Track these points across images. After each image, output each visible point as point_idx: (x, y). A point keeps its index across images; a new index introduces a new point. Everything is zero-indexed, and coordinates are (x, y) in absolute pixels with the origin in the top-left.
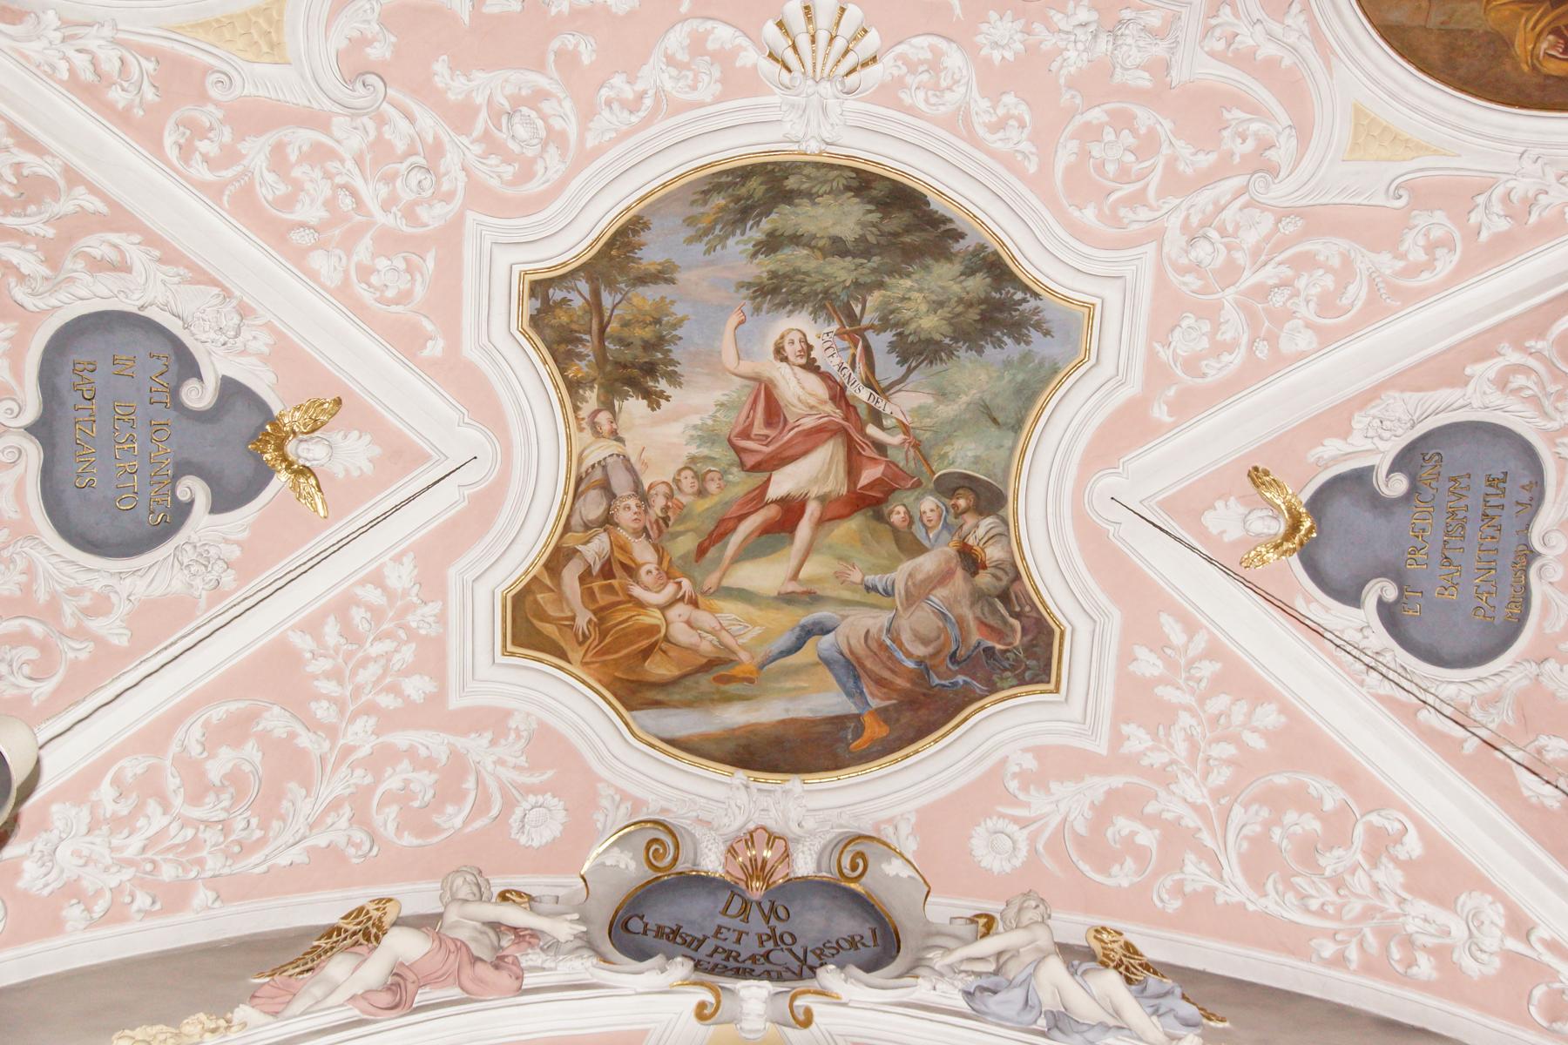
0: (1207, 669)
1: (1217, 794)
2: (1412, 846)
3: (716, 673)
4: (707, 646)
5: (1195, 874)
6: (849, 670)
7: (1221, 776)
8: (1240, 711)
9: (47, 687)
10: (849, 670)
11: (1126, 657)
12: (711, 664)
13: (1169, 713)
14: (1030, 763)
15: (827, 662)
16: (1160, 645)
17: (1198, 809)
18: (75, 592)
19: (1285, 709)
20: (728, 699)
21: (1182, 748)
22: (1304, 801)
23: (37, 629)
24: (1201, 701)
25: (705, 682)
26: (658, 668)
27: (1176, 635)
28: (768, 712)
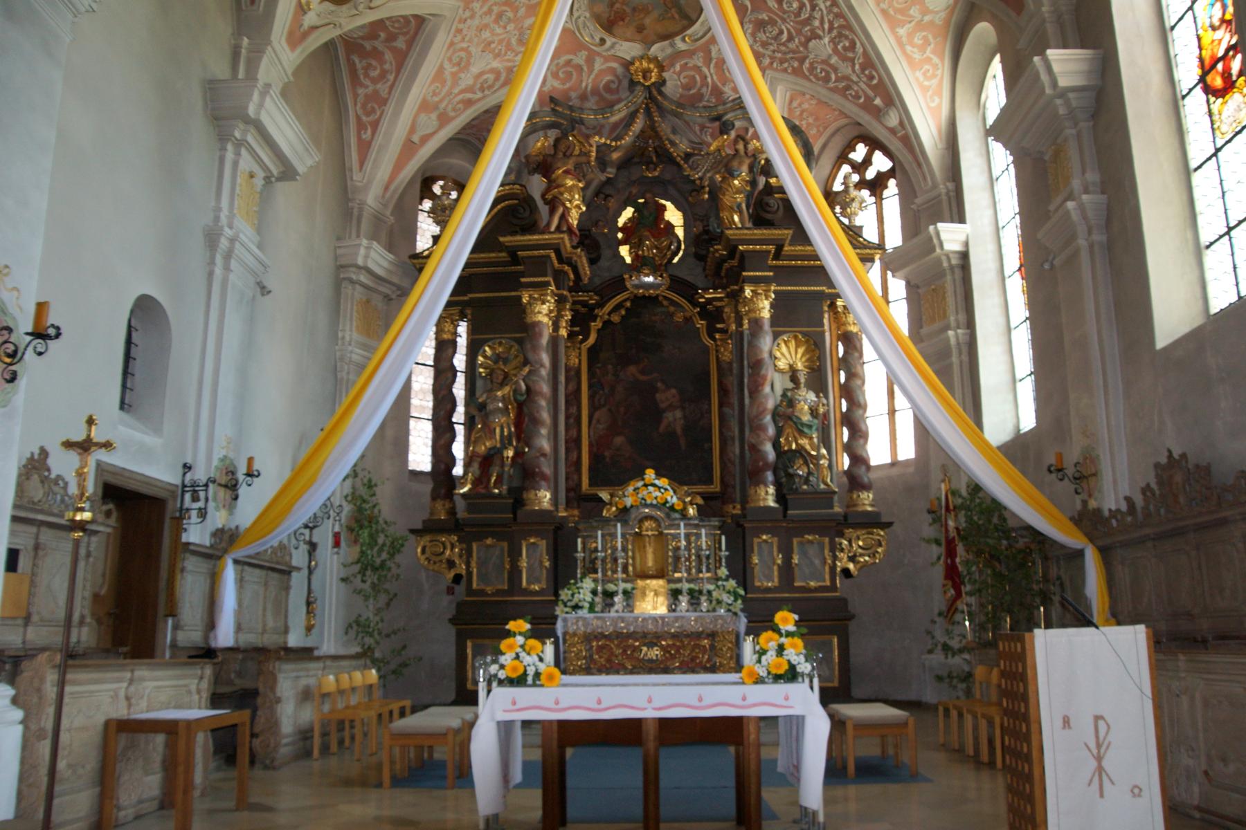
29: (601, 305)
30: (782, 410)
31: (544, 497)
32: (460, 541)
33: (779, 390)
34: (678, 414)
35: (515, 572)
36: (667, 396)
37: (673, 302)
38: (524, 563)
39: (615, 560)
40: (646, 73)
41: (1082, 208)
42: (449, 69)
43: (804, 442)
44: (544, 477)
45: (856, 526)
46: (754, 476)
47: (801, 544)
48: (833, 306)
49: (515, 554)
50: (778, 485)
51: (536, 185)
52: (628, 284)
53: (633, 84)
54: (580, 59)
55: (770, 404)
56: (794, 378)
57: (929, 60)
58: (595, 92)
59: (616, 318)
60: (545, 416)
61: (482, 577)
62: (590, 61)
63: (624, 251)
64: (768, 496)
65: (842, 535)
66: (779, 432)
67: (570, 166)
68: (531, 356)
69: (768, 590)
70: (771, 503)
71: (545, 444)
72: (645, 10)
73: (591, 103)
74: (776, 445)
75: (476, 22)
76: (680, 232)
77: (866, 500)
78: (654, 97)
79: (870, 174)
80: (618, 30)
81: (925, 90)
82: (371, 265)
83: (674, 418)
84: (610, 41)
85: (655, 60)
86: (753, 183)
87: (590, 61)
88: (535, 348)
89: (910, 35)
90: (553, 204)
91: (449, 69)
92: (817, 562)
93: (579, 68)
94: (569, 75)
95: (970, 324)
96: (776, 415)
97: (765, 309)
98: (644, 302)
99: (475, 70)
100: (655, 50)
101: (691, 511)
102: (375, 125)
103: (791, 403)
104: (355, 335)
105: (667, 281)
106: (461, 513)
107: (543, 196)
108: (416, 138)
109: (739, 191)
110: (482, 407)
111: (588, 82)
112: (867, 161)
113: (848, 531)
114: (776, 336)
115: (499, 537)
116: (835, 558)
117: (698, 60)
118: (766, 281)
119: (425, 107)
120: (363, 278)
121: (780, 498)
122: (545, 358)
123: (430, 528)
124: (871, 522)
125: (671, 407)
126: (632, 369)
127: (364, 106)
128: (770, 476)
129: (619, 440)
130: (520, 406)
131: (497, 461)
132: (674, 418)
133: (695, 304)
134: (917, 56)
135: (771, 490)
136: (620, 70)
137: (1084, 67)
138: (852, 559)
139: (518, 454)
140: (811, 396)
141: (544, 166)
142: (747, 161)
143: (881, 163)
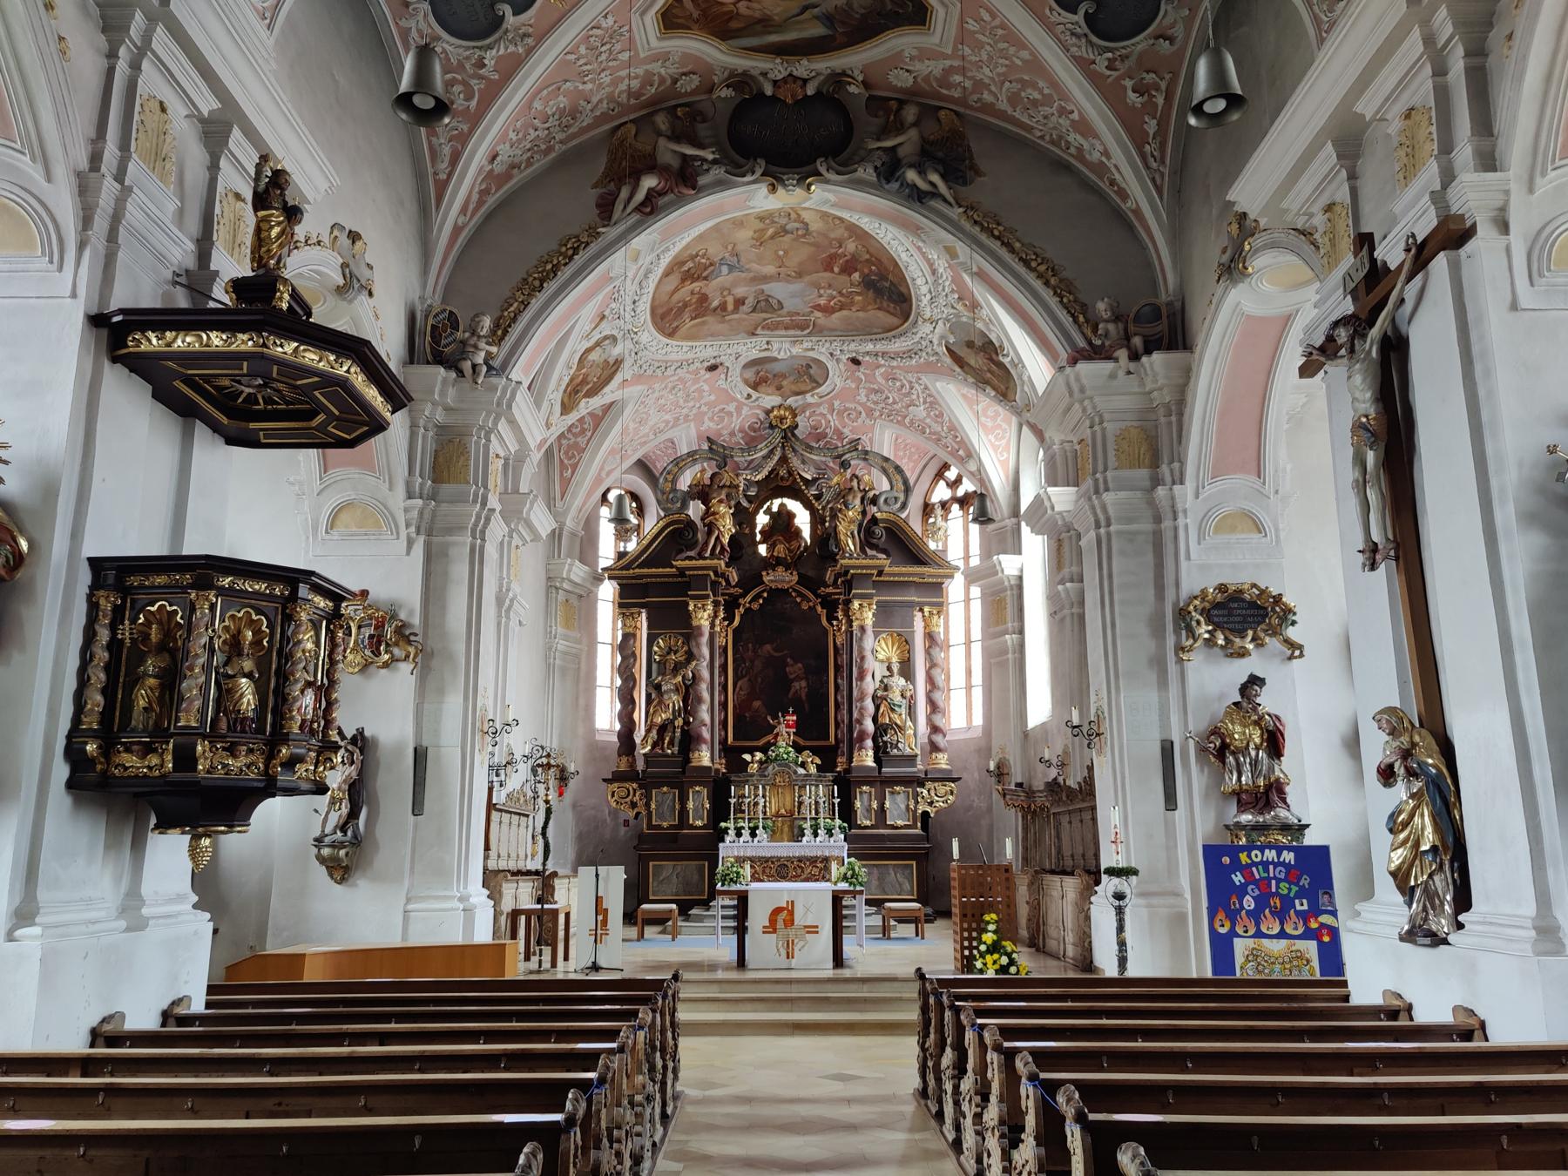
0: (1000, 32)
1: (999, 75)
2: (1075, 116)
3: (765, 24)
4: (757, 15)
5: (987, 97)
6: (828, 19)
7: (1001, 70)
8: (1012, 50)
9: (474, 103)
10: (828, 19)
11: (962, 21)
12: (760, 21)
13: (981, 46)
14: (915, 52)
15: (816, 17)
16: (979, 20)
17: (992, 79)
18: (467, 58)
19: (1032, 54)
20: (770, 33)
21: (985, 57)
22: (1034, 86)
23: (459, 77)
24: (996, 42)
25: (758, 28)
26: (734, 25)
27: (987, 17)
28: (790, 36)
29: (744, 595)
30: (880, 693)
31: (704, 757)
32: (641, 787)
33: (878, 678)
34: (803, 683)
35: (683, 812)
36: (795, 669)
37: (800, 594)
38: (690, 805)
39: (756, 804)
40: (782, 419)
41: (1067, 591)
42: (632, 426)
43: (895, 717)
44: (705, 742)
45: (934, 780)
46: (854, 742)
47: (892, 793)
48: (921, 610)
49: (683, 800)
50: (876, 749)
51: (695, 510)
52: (766, 579)
53: (771, 427)
54: (732, 407)
55: (871, 691)
56: (889, 668)
57: (999, 426)
58: (741, 431)
59: (755, 606)
60: (706, 695)
61: (661, 816)
62: (739, 409)
63: (763, 549)
64: (867, 758)
65: (923, 786)
66: (877, 708)
67: (723, 497)
68: (695, 650)
69: (866, 827)
70: (870, 762)
71: (706, 717)
72: (784, 376)
73: (739, 437)
74: (875, 719)
75: (656, 394)
76: (806, 534)
77: (942, 761)
78: (789, 435)
79: (960, 492)
80: (763, 388)
81: (996, 448)
82: (573, 577)
83: (800, 686)
84: (755, 395)
85: (789, 408)
86: (864, 513)
87: (739, 409)
88: (698, 645)
89: (984, 410)
90: (711, 528)
91: (632, 426)
92: (903, 806)
93: (730, 414)
94: (722, 419)
95: (1021, 632)
96: (874, 698)
97: (869, 617)
98: (778, 594)
99: (651, 423)
100: (791, 401)
101: (813, 770)
102: (575, 467)
103: (886, 688)
104: (560, 630)
105: (795, 578)
106: (640, 765)
107: (703, 519)
108: (603, 474)
109: (852, 522)
110: (658, 687)
111: (736, 423)
112: (958, 481)
113: (929, 785)
114: (876, 634)
115: (672, 786)
116: (917, 802)
117: (824, 410)
118: (869, 597)
119: (612, 452)
120: (565, 586)
121: (877, 759)
122: (706, 651)
123: (618, 777)
124: (946, 778)
125: (798, 678)
126: (768, 647)
127: (566, 453)
128: (869, 743)
129: (757, 704)
130: (687, 688)
131: (670, 728)
132: (800, 686)
133: (817, 596)
134: (990, 424)
135: (871, 753)
136: (762, 416)
137: (1073, 498)
138: (931, 804)
139: (686, 723)
140: (902, 681)
141: (702, 492)
142: (860, 495)
143: (967, 486)
